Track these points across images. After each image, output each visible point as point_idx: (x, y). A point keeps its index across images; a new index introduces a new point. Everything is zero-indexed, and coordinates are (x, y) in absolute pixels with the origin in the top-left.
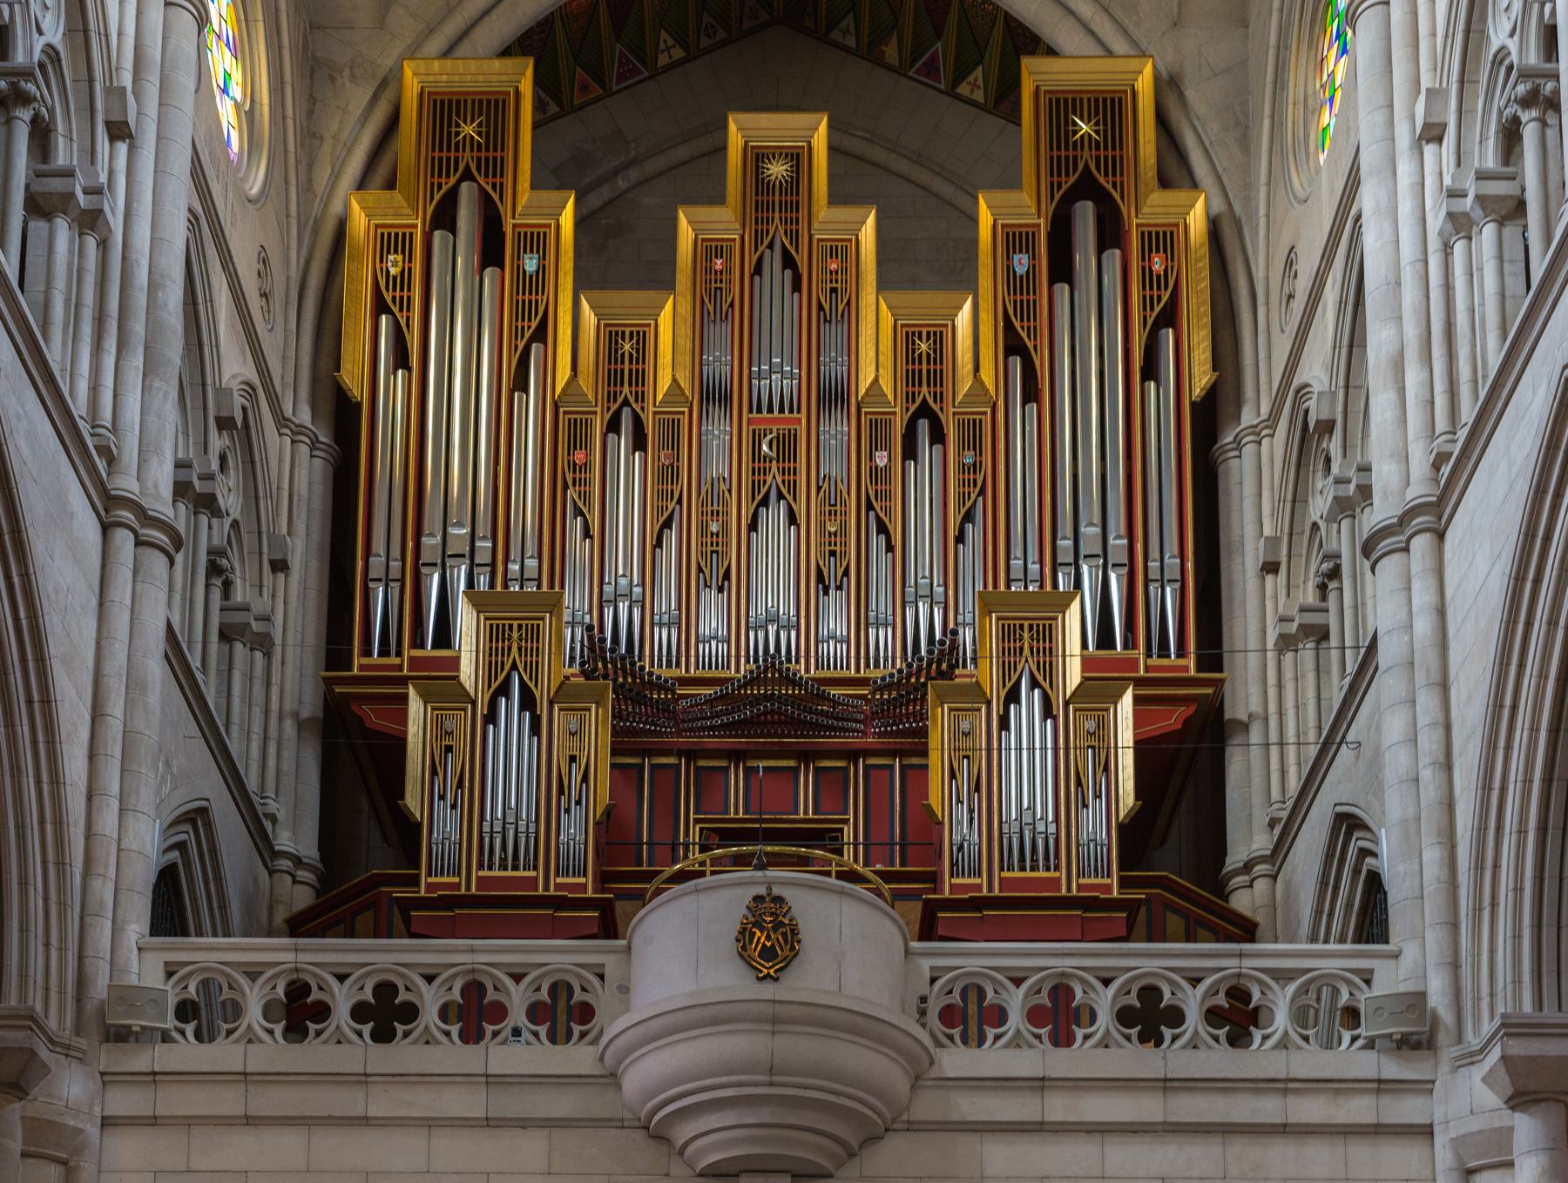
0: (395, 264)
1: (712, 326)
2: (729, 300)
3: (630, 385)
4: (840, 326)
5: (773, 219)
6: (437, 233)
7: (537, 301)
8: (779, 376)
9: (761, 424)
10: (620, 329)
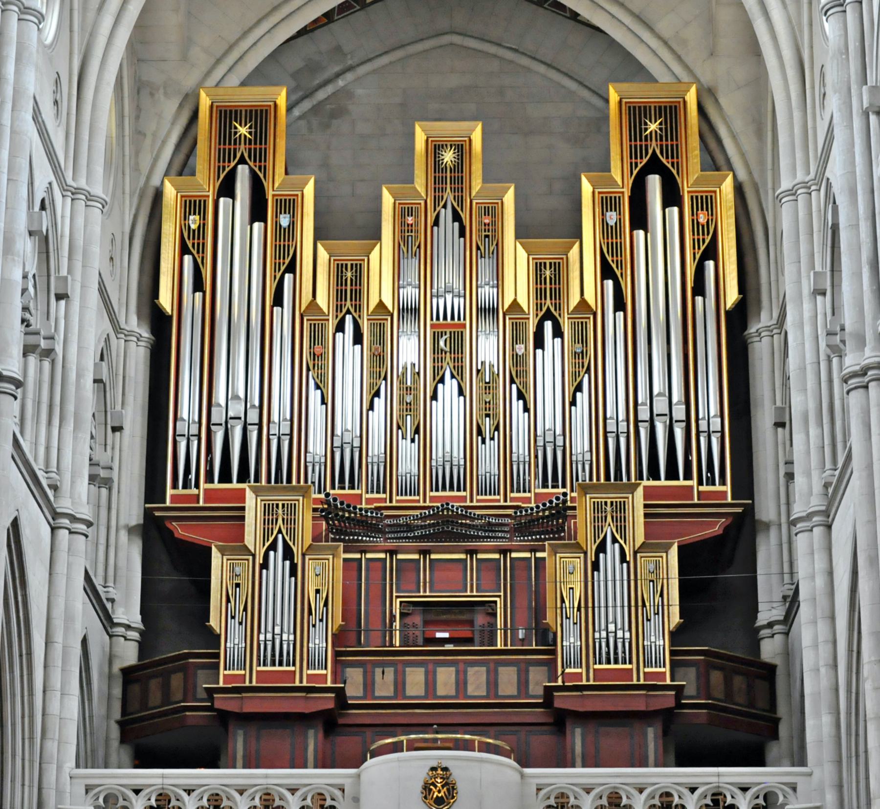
1: (406, 260)
2: (417, 244)
3: (351, 300)
4: (491, 260)
5: (446, 188)
6: (222, 200)
7: (289, 246)
8: (451, 295)
9: (439, 328)
10: (344, 262)
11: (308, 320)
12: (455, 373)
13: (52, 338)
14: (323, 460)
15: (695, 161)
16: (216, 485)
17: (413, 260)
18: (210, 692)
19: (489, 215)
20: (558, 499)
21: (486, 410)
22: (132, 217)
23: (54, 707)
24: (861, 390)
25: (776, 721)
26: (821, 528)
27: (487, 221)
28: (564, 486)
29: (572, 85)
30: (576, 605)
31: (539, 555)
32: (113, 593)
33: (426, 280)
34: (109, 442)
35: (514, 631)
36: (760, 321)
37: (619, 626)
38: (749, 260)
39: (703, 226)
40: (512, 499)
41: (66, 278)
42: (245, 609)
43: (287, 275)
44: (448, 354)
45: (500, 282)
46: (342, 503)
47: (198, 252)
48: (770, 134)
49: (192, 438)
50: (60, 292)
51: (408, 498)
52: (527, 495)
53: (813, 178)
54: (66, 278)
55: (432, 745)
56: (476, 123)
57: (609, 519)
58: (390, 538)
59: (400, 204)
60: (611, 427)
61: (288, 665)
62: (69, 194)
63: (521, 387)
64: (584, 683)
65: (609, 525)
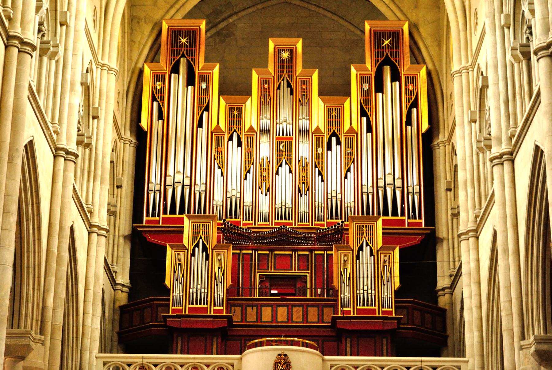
0: (159, 85)
1: (264, 106)
2: (269, 98)
3: (236, 125)
4: (306, 106)
5: (284, 71)
6: (173, 75)
7: (206, 98)
9: (280, 140)
10: (233, 107)
11: (215, 135)
12: (288, 162)
13: (90, 138)
14: (221, 204)
15: (408, 59)
16: (168, 216)
17: (267, 106)
18: (165, 317)
19: (305, 84)
20: (339, 224)
21: (303, 180)
22: (128, 82)
23: (89, 322)
24: (499, 166)
25: (447, 337)
26: (474, 238)
27: (304, 87)
28: (341, 218)
29: (345, 23)
30: (348, 276)
31: (328, 252)
32: (116, 268)
33: (274, 116)
34: (115, 193)
35: (316, 291)
36: (438, 138)
37: (369, 287)
38: (434, 107)
39: (411, 91)
40: (315, 225)
41: (97, 108)
42: (183, 276)
43: (205, 112)
44: (284, 152)
45: (310, 118)
46: (231, 225)
47: (161, 100)
48: (445, 46)
49: (156, 192)
50: (95, 115)
51: (264, 223)
52: (323, 222)
53: (470, 64)
54: (97, 108)
55: (278, 343)
56: (299, 39)
57: (365, 234)
58: (254, 243)
59: (261, 78)
60: (365, 190)
61: (204, 304)
62: (100, 67)
63: (320, 169)
64: (352, 315)
65: (365, 237)
